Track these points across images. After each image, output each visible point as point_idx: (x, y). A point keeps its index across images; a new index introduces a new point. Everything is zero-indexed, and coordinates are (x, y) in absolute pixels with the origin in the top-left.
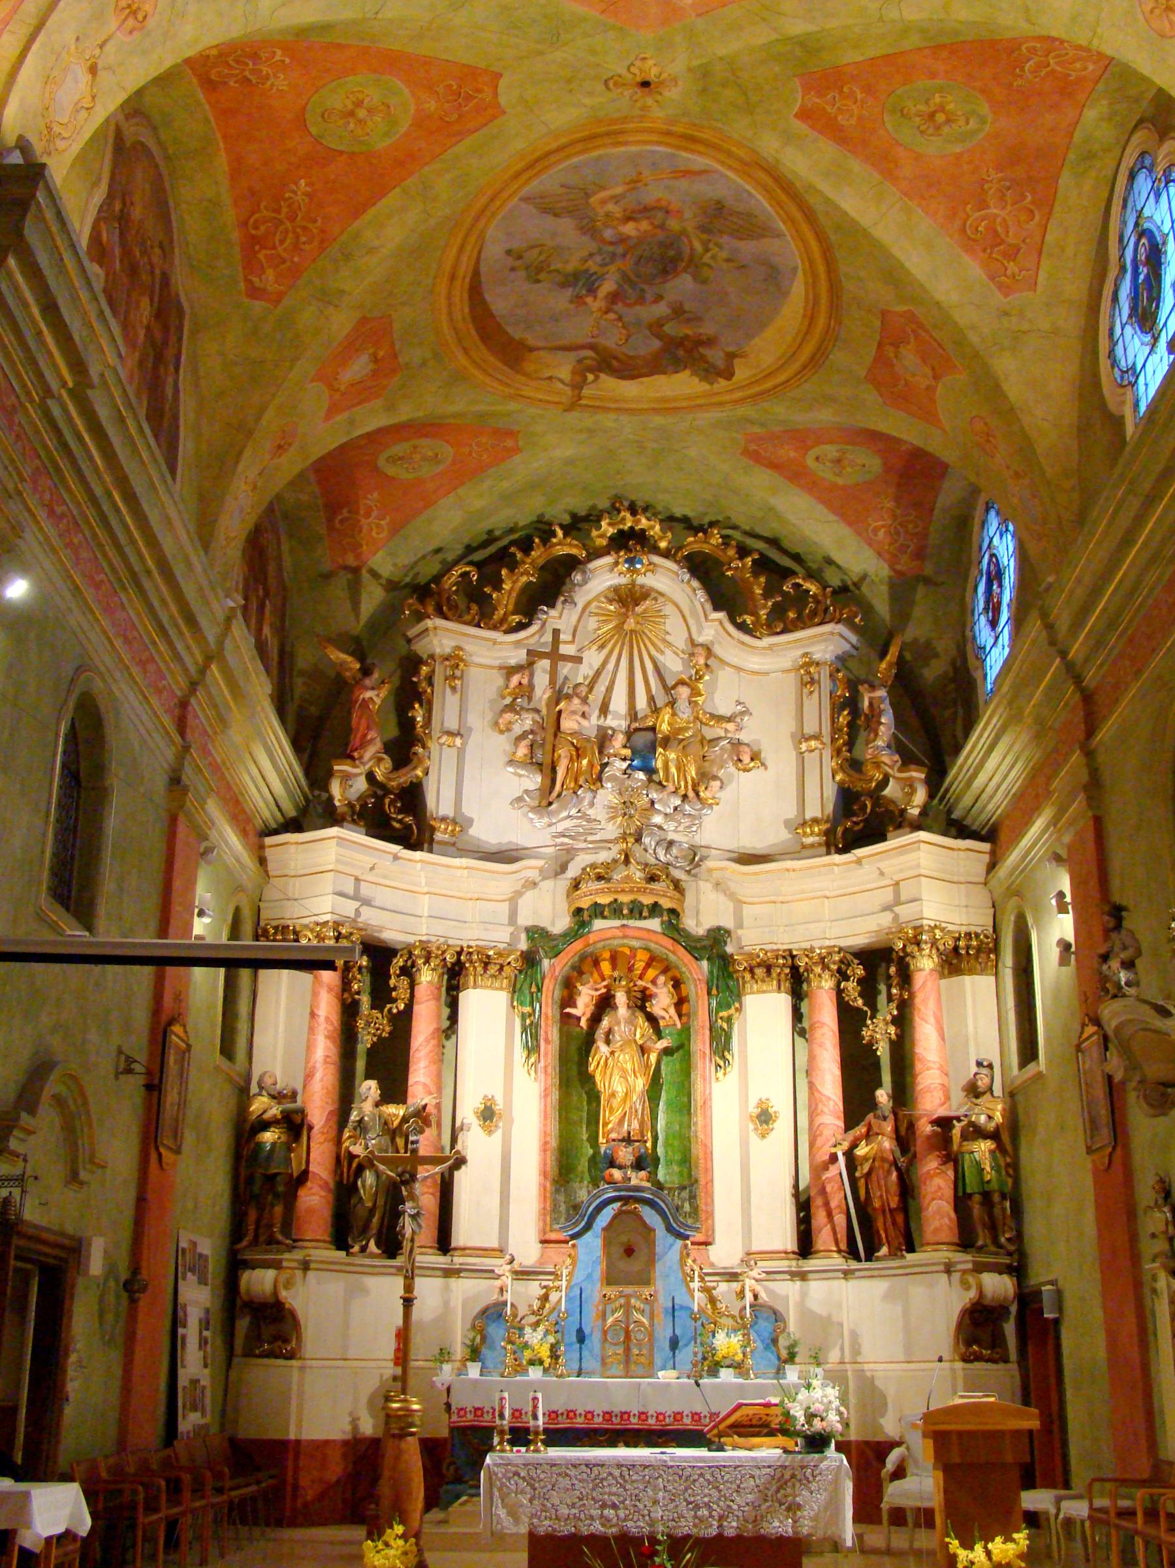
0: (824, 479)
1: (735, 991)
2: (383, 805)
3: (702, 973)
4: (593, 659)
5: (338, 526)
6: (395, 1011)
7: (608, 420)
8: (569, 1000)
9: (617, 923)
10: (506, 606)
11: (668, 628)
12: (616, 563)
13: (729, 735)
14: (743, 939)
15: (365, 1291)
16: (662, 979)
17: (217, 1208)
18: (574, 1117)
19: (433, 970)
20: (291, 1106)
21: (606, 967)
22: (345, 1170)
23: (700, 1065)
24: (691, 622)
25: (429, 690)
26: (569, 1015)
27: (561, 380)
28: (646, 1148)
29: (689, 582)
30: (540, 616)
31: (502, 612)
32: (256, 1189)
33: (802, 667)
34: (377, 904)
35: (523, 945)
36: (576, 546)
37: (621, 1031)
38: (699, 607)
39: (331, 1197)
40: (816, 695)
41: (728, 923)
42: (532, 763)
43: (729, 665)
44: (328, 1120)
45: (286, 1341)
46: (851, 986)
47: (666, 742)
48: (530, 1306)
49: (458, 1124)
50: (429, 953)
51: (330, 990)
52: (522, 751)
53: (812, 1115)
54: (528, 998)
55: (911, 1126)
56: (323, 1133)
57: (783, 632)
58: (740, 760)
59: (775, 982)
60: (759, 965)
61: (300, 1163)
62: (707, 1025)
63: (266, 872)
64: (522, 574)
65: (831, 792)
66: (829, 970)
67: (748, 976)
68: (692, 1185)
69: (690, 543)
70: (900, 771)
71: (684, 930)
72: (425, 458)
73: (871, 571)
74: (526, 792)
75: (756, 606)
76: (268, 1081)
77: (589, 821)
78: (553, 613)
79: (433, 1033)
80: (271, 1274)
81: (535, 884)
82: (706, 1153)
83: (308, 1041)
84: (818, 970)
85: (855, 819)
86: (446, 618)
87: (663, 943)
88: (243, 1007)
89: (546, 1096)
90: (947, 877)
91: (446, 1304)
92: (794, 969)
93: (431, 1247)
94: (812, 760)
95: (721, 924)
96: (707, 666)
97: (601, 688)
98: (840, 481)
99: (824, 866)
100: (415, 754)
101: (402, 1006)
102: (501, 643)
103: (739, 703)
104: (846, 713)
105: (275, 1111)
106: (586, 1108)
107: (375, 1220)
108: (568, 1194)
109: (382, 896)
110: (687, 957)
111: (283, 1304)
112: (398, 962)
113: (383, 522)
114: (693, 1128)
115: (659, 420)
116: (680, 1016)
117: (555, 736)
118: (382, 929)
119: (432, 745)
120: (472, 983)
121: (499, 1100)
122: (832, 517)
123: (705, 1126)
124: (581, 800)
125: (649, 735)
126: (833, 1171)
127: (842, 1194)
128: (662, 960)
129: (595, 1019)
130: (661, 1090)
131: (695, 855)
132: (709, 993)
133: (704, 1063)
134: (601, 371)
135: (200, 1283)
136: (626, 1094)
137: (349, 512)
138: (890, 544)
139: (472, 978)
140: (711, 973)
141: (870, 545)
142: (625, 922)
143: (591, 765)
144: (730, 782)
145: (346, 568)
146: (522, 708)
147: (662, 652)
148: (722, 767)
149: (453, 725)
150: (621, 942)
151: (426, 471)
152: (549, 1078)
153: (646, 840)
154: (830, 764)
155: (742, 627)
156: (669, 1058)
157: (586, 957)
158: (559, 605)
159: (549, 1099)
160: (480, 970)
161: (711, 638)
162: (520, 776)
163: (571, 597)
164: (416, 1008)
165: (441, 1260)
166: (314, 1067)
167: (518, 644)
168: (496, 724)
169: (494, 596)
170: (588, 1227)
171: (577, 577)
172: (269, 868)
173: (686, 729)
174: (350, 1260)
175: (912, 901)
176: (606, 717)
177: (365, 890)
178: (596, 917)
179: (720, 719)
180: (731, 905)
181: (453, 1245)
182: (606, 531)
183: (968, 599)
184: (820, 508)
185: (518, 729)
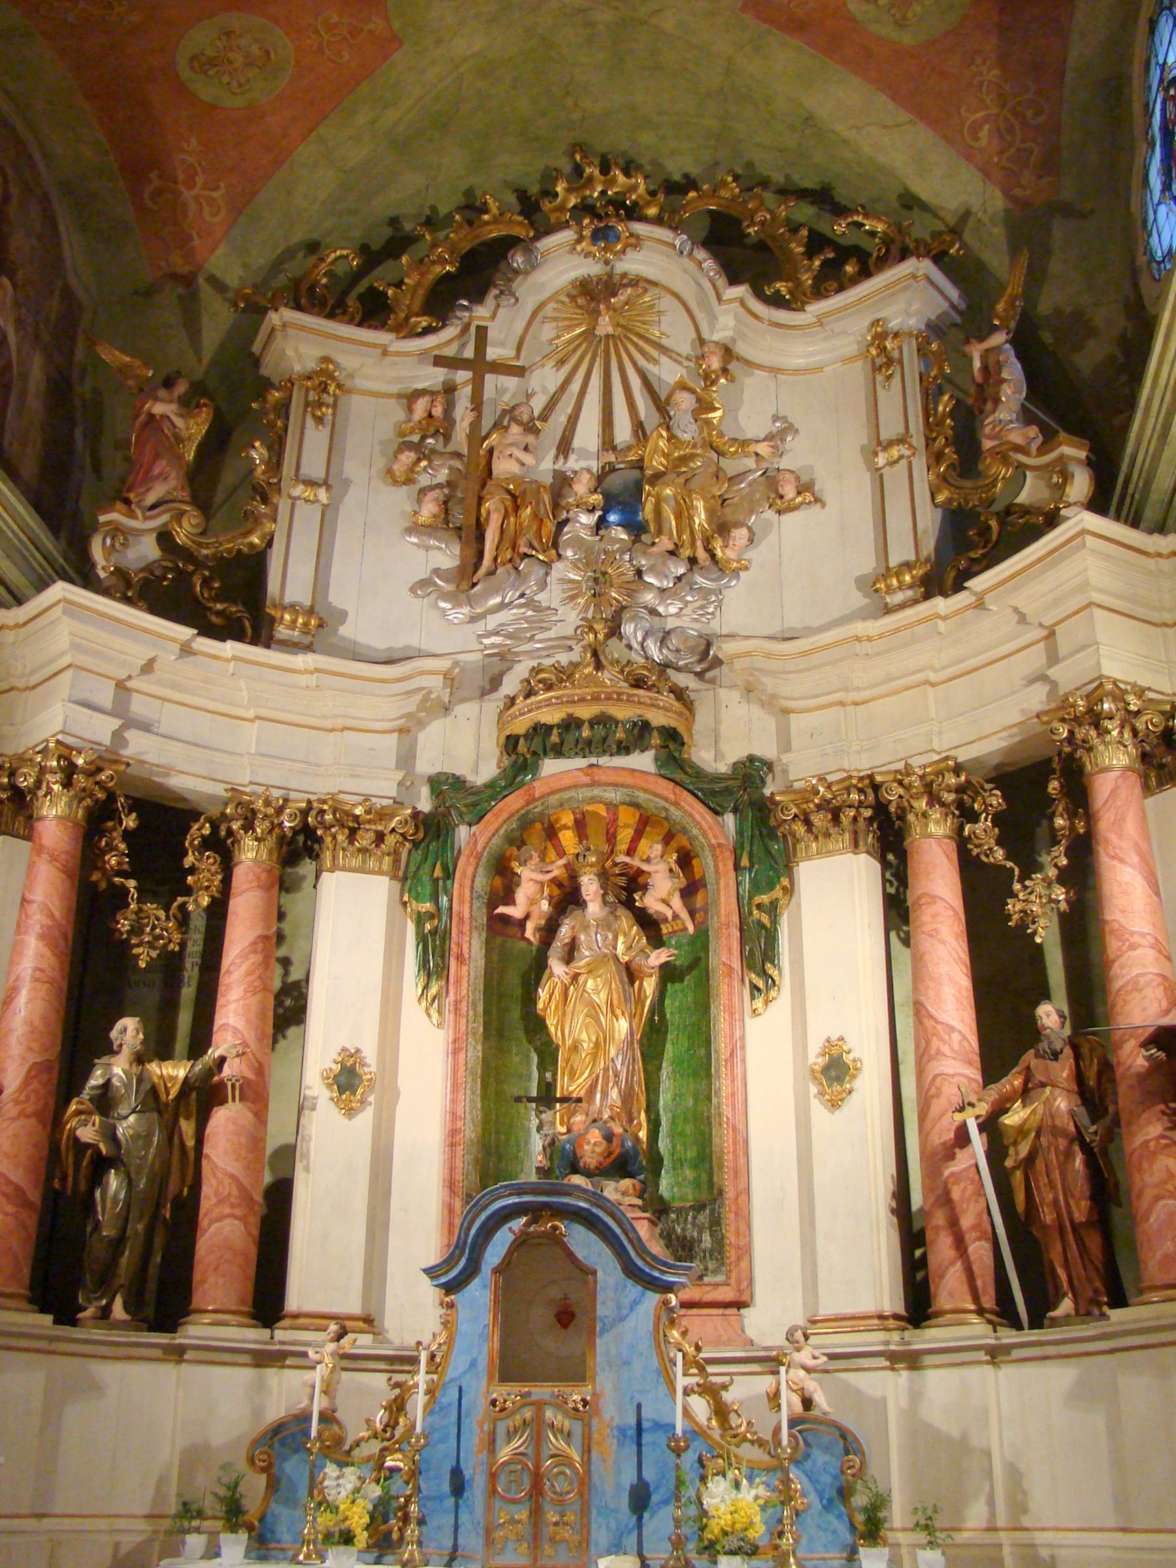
1: (781, 860)
2: (192, 587)
3: (727, 838)
4: (545, 379)
9: (580, 763)
10: (409, 307)
11: (664, 327)
12: (579, 240)
13: (764, 465)
14: (791, 769)
15: (96, 1388)
19: (257, 839)
21: (568, 838)
22: (70, 1172)
23: (724, 988)
24: (700, 316)
25: (279, 423)
26: (505, 919)
28: (637, 1139)
29: (690, 254)
30: (459, 314)
31: (402, 315)
33: (871, 344)
34: (161, 731)
35: (425, 805)
36: (520, 223)
38: (707, 286)
39: (32, 1221)
40: (896, 382)
41: (766, 750)
42: (448, 529)
43: (760, 367)
46: (983, 830)
47: (657, 477)
50: (254, 812)
51: (53, 858)
52: (429, 509)
53: (923, 1057)
54: (428, 889)
55: (1107, 1069)
57: (841, 289)
58: (782, 497)
59: (847, 836)
64: (434, 263)
65: (930, 520)
66: (943, 804)
67: (800, 829)
68: (715, 1200)
69: (693, 200)
70: (1041, 451)
71: (693, 766)
72: (249, 63)
73: (975, 204)
74: (436, 571)
75: (796, 271)
78: (481, 312)
79: (254, 943)
81: (447, 709)
82: (735, 1143)
84: (922, 804)
85: (973, 555)
86: (299, 307)
87: (659, 791)
89: (455, 1052)
90: (1139, 611)
92: (880, 808)
94: (896, 478)
95: (758, 753)
96: (725, 371)
97: (560, 418)
98: (907, 39)
99: (920, 622)
102: (398, 354)
103: (776, 418)
104: (946, 398)
109: (170, 719)
112: (201, 829)
114: (714, 1100)
116: (692, 914)
117: (483, 485)
118: (168, 771)
119: (283, 505)
121: (370, 1055)
122: (903, 116)
126: (962, 1161)
127: (982, 1204)
131: (709, 645)
132: (737, 867)
133: (730, 985)
136: (597, 1044)
138: (1001, 152)
140: (740, 832)
141: (968, 157)
142: (593, 760)
146: (433, 451)
147: (656, 362)
148: (751, 512)
149: (319, 474)
152: (464, 1021)
153: (628, 629)
154: (923, 479)
155: (777, 301)
156: (677, 986)
157: (532, 822)
158: (490, 300)
159: (462, 1055)
161: (730, 333)
162: (427, 548)
165: (253, 1336)
167: (422, 354)
168: (389, 471)
169: (390, 292)
171: (518, 260)
175: (1078, 651)
176: (566, 458)
177: (139, 706)
178: (545, 754)
179: (744, 443)
180: (771, 723)
182: (565, 200)
183: (1134, 207)
184: (882, 100)
185: (424, 480)
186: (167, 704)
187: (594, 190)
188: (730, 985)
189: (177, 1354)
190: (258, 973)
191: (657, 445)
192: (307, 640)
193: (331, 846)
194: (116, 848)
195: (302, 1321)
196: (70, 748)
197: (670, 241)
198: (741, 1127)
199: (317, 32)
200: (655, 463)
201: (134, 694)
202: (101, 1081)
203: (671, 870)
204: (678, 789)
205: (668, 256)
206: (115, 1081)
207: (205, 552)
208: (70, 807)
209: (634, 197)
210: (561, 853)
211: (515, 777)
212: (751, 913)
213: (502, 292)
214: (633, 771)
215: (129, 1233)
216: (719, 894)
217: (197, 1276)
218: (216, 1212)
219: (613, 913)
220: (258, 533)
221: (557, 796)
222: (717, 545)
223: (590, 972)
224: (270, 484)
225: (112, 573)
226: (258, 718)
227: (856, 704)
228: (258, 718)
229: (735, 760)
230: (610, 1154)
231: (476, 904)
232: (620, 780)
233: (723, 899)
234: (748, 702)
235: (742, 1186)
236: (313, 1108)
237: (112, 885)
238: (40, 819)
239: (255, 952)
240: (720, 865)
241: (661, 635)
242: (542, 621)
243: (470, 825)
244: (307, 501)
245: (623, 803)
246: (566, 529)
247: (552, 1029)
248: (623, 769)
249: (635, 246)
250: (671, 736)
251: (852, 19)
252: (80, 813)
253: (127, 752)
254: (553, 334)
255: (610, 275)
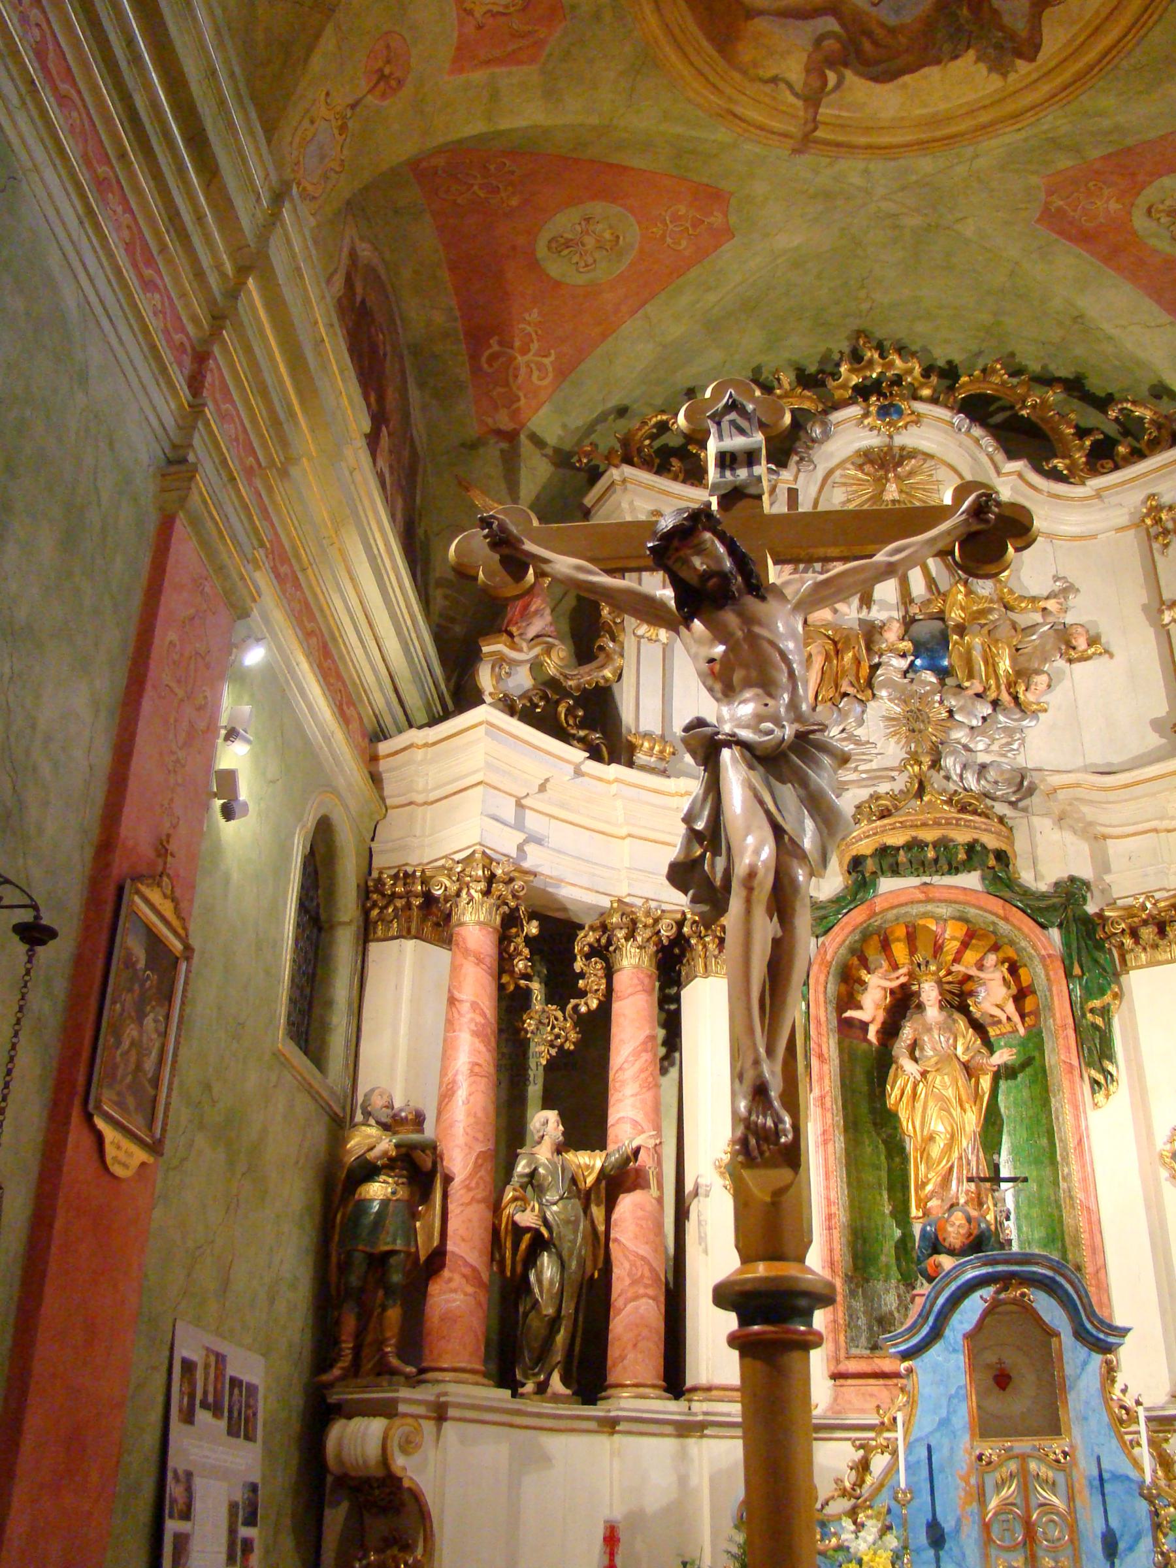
0: (1155, 251)
2: (556, 714)
5: (485, 366)
6: (583, 1009)
7: (852, 169)
8: (848, 998)
9: (913, 881)
12: (866, 415)
15: (546, 1460)
16: (992, 959)
17: (281, 1306)
18: (869, 1177)
19: (640, 947)
20: (415, 1137)
21: (900, 950)
22: (508, 1254)
23: (1066, 1084)
27: (790, 87)
28: (987, 1222)
29: (969, 430)
32: (354, 1280)
33: (1148, 515)
36: (809, 398)
37: (934, 1044)
38: (985, 460)
41: (1085, 872)
44: (477, 1167)
45: (407, 1548)
47: (961, 630)
48: (838, 1481)
49: (689, 1187)
51: (479, 961)
56: (468, 1188)
57: (1117, 468)
58: (1074, 648)
60: (1145, 923)
61: (430, 1237)
62: (1071, 1021)
63: (383, 799)
67: (1128, 942)
71: (1020, 886)
75: (1069, 450)
76: (378, 1102)
77: (858, 743)
78: (786, 475)
79: (644, 1043)
80: (376, 1425)
82: (1090, 1223)
83: (445, 1040)
87: (989, 908)
88: (341, 989)
91: (683, 1481)
93: (654, 1386)
95: (1076, 873)
100: (601, 648)
101: (594, 1004)
105: (386, 1144)
106: (885, 1165)
107: (561, 1338)
108: (871, 1299)
109: (558, 834)
110: (1028, 924)
111: (400, 1480)
113: (546, 361)
114: (1063, 1185)
115: (925, 165)
116: (1022, 1016)
118: (560, 881)
119: (629, 642)
120: (701, 968)
123: (1084, 1179)
124: (844, 715)
125: (938, 625)
128: (984, 936)
129: (890, 1030)
130: (1000, 1132)
131: (1023, 778)
132: (1068, 975)
133: (1072, 1082)
134: (846, 65)
135: (232, 1432)
136: (952, 1136)
137: (500, 343)
139: (701, 961)
140: (1067, 944)
142: (927, 879)
143: (858, 662)
144: (1060, 681)
145: (499, 433)
150: (922, 908)
151: (605, 271)
152: (829, 1115)
153: (948, 762)
155: (1055, 476)
157: (871, 934)
159: (830, 1147)
160: (711, 947)
163: (809, 455)
164: (616, 1006)
165: (672, 1408)
166: (454, 1082)
170: (936, 1334)
172: (386, 792)
173: (990, 611)
174: (517, 1404)
176: (869, 608)
177: (533, 822)
178: (883, 873)
179: (1034, 599)
180: (1084, 847)
181: (689, 1382)
182: (848, 380)
186: (553, 821)
187: (872, 370)
188: (1072, 1082)
189: (610, 1425)
190: (650, 1069)
191: (956, 600)
192: (662, 765)
193: (702, 954)
194: (520, 954)
195: (714, 1393)
196: (491, 860)
197: (948, 419)
198: (1094, 1207)
199: (664, 222)
200: (953, 615)
201: (527, 811)
202: (527, 1170)
203: (1004, 978)
204: (1008, 905)
205: (946, 432)
206: (541, 1170)
207: (570, 683)
208: (490, 913)
209: (909, 380)
210: (895, 967)
211: (856, 894)
212: (1084, 1016)
213: (802, 459)
214: (965, 889)
215: (563, 1313)
216: (1052, 999)
217: (613, 1352)
218: (630, 1294)
219: (950, 1016)
220: (610, 668)
221: (895, 911)
222: (1021, 689)
223: (938, 1070)
224: (615, 623)
225: (500, 700)
226: (630, 835)
227: (1169, 831)
228: (630, 835)
229: (1054, 880)
230: (971, 1234)
231: (830, 1008)
232: (952, 897)
233: (1056, 1002)
234: (1061, 828)
235: (1100, 1263)
236: (707, 1196)
237: (517, 987)
238: (461, 924)
239: (646, 1051)
240: (1051, 973)
241: (977, 768)
242: (864, 754)
243: (817, 937)
244: (650, 640)
245: (953, 918)
246: (879, 672)
247: (905, 1124)
248: (957, 888)
249: (917, 422)
250: (1002, 857)
251: (1134, 233)
252: (498, 919)
253: (526, 865)
254: (843, 498)
255: (890, 447)
